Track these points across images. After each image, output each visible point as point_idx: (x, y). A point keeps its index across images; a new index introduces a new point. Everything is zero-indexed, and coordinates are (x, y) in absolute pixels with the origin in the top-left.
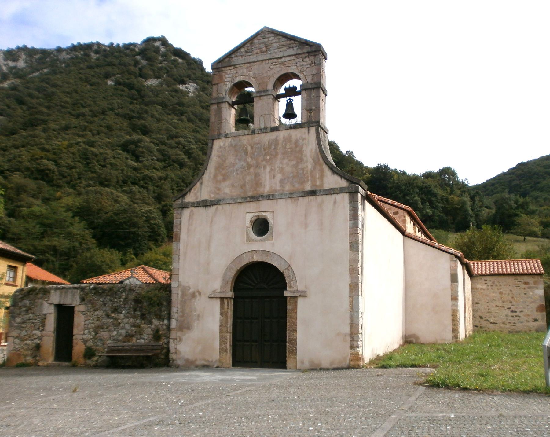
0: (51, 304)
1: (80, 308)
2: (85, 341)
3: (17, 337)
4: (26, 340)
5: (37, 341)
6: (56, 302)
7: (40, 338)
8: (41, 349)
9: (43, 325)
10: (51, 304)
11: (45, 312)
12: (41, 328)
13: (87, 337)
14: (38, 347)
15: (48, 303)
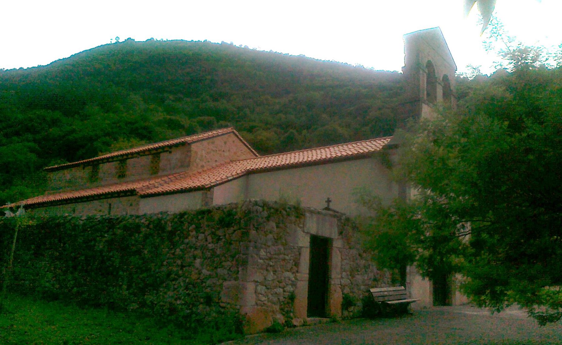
0: (307, 233)
1: (337, 244)
2: (343, 287)
3: (262, 284)
4: (275, 287)
5: (289, 288)
6: (314, 231)
7: (294, 285)
8: (296, 301)
9: (297, 264)
10: (307, 233)
11: (300, 245)
12: (295, 269)
13: (346, 281)
14: (292, 298)
15: (304, 232)
